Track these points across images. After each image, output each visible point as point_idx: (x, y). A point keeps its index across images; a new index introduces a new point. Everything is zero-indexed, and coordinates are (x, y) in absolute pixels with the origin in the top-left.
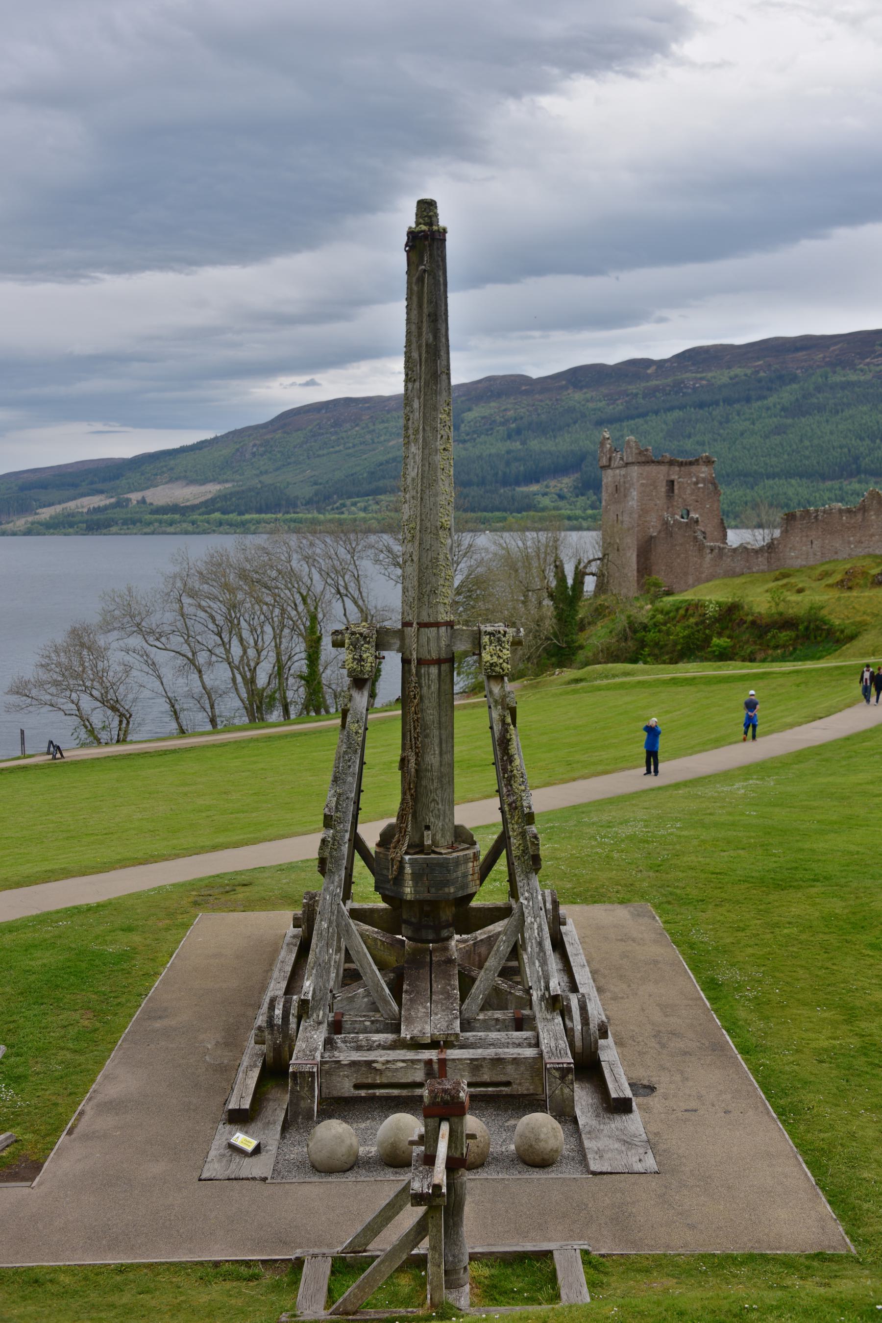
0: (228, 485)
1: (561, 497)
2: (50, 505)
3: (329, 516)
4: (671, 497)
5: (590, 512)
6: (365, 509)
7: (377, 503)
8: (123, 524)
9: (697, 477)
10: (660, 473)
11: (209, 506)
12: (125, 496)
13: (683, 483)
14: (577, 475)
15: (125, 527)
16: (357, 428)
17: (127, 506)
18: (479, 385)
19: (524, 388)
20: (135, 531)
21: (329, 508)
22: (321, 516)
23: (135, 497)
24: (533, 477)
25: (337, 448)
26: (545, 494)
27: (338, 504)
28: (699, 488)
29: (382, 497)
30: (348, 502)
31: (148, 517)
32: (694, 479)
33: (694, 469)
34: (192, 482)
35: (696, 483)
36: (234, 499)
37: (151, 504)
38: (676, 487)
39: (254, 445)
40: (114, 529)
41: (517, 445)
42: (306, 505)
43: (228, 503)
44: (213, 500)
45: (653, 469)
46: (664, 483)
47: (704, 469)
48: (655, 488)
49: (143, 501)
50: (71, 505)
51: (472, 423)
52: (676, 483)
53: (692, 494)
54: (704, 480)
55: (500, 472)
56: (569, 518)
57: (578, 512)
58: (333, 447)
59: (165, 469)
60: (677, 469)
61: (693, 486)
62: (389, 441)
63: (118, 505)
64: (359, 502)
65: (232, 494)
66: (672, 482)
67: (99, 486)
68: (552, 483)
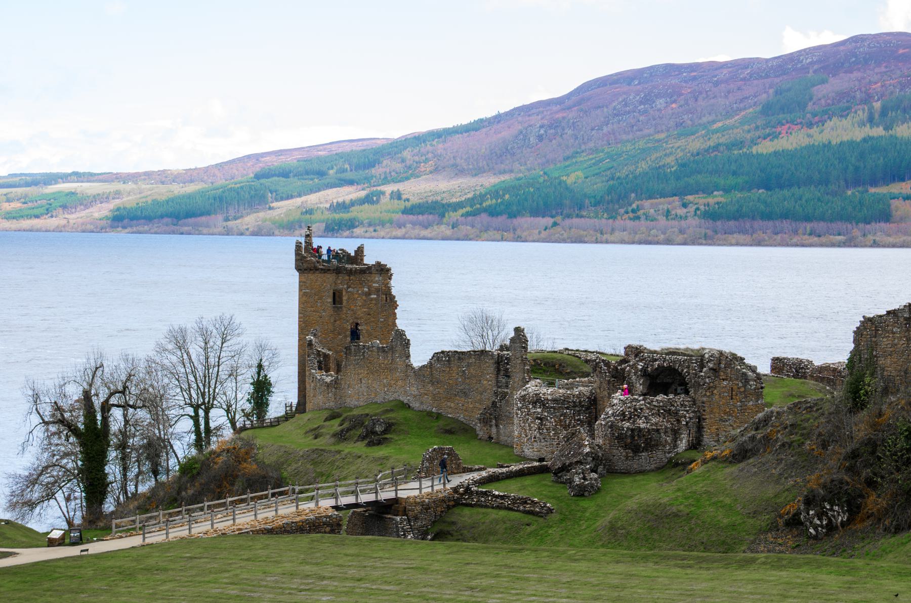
4: (338, 308)
7: (685, 205)
8: (370, 225)
9: (369, 287)
10: (328, 282)
12: (379, 188)
13: (353, 293)
15: (371, 229)
16: (674, 105)
17: (378, 201)
18: (842, 48)
19: (901, 51)
20: (382, 234)
21: (622, 211)
25: (646, 132)
27: (634, 206)
28: (372, 299)
29: (690, 198)
30: (647, 204)
32: (366, 290)
33: (366, 276)
34: (460, 172)
35: (368, 294)
36: (507, 196)
37: (408, 200)
38: (345, 298)
39: (542, 127)
41: (879, 131)
42: (595, 205)
43: (499, 201)
48: (321, 298)
51: (823, 102)
53: (363, 306)
54: (378, 291)
55: (851, 167)
58: (641, 130)
59: (430, 155)
61: (364, 297)
62: (714, 122)
63: (368, 200)
64: (660, 204)
65: (506, 190)
66: (340, 292)
67: (349, 175)
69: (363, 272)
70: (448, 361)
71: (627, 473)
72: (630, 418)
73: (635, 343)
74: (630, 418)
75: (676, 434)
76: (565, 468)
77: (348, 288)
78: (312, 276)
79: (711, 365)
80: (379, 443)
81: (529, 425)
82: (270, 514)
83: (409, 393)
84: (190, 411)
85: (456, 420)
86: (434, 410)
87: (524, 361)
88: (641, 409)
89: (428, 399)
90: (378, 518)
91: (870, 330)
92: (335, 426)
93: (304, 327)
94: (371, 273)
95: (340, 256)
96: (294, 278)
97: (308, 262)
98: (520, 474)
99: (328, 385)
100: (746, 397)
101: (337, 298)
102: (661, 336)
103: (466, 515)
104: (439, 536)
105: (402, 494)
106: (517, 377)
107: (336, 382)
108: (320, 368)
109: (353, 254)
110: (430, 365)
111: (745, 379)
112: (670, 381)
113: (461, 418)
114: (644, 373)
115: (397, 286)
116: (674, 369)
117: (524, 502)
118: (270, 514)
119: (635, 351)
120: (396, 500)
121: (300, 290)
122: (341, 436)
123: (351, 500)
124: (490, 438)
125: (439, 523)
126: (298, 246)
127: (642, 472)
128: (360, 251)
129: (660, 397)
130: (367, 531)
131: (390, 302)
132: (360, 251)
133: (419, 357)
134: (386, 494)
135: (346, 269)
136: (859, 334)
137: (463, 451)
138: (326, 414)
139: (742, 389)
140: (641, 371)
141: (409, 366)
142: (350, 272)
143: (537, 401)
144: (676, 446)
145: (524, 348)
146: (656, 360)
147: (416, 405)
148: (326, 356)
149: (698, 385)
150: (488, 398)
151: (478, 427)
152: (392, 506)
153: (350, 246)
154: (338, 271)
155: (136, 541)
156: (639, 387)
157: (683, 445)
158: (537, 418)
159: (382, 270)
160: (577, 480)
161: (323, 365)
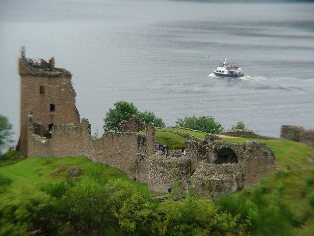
9: (61, 84)
10: (37, 82)
33: (58, 79)
45: (31, 80)
46: (39, 88)
47: (65, 79)
52: (46, 88)
54: (65, 87)
60: (47, 79)
69: (56, 76)
70: (112, 137)
72: (208, 175)
74: (208, 175)
77: (49, 84)
78: (28, 78)
79: (249, 148)
81: (157, 176)
83: (90, 153)
86: (104, 162)
88: (214, 170)
93: (24, 105)
94: (61, 77)
99: (44, 145)
100: (266, 164)
101: (42, 90)
107: (48, 144)
108: (36, 133)
109: (48, 62)
112: (228, 154)
113: (118, 167)
115: (75, 82)
116: (231, 149)
121: (22, 86)
124: (135, 179)
128: (52, 61)
129: (224, 164)
131: (71, 93)
132: (52, 61)
135: (47, 75)
138: (44, 161)
139: (264, 160)
140: (214, 149)
141: (91, 138)
142: (50, 76)
145: (154, 134)
146: (221, 144)
147: (94, 160)
148: (39, 125)
150: (133, 158)
151: (129, 172)
156: (213, 157)
158: (163, 172)
159: (68, 75)
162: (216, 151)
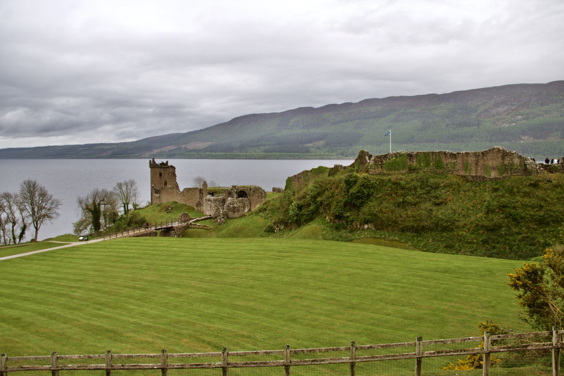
0: (213, 143)
1: (318, 148)
2: (156, 149)
3: (242, 154)
5: (327, 153)
6: (255, 151)
10: (158, 171)
11: (206, 150)
14: (324, 141)
22: (240, 154)
23: (183, 146)
24: (310, 141)
26: (313, 147)
30: (249, 149)
31: (186, 153)
33: (168, 169)
40: (175, 157)
41: (306, 131)
44: (207, 148)
45: (156, 170)
49: (186, 148)
50: (163, 149)
54: (171, 173)
56: (320, 155)
57: (323, 153)
63: (178, 149)
68: (316, 143)
71: (232, 218)
73: (235, 185)
75: (244, 207)
76: (216, 217)
78: (154, 169)
80: (170, 212)
82: (138, 232)
84: (123, 205)
85: (189, 206)
87: (206, 190)
89: (182, 200)
90: (167, 232)
91: (290, 181)
92: (159, 208)
95: (163, 164)
96: (150, 169)
97: (153, 165)
98: (205, 219)
101: (160, 175)
102: (242, 183)
103: (190, 230)
104: (183, 236)
105: (173, 225)
106: (205, 194)
110: (183, 191)
111: (262, 193)
113: (191, 205)
114: (236, 192)
117: (205, 226)
118: (138, 232)
119: (234, 187)
120: (172, 227)
122: (160, 211)
123: (160, 227)
125: (183, 233)
126: (150, 162)
127: (235, 218)
128: (167, 162)
129: (240, 198)
130: (164, 236)
131: (174, 175)
132: (167, 162)
133: (181, 189)
134: (170, 226)
136: (287, 181)
137: (191, 215)
142: (164, 168)
143: (209, 200)
144: (244, 211)
147: (180, 202)
149: (250, 195)
150: (198, 200)
152: (171, 229)
153: (164, 161)
154: (161, 167)
155: (102, 239)
156: (235, 196)
157: (246, 210)
160: (219, 220)
161: (157, 192)
162: (236, 192)
